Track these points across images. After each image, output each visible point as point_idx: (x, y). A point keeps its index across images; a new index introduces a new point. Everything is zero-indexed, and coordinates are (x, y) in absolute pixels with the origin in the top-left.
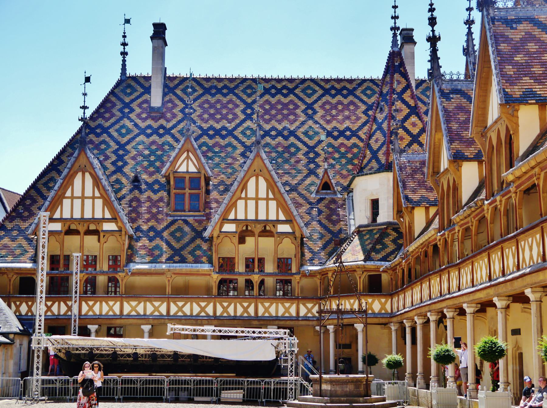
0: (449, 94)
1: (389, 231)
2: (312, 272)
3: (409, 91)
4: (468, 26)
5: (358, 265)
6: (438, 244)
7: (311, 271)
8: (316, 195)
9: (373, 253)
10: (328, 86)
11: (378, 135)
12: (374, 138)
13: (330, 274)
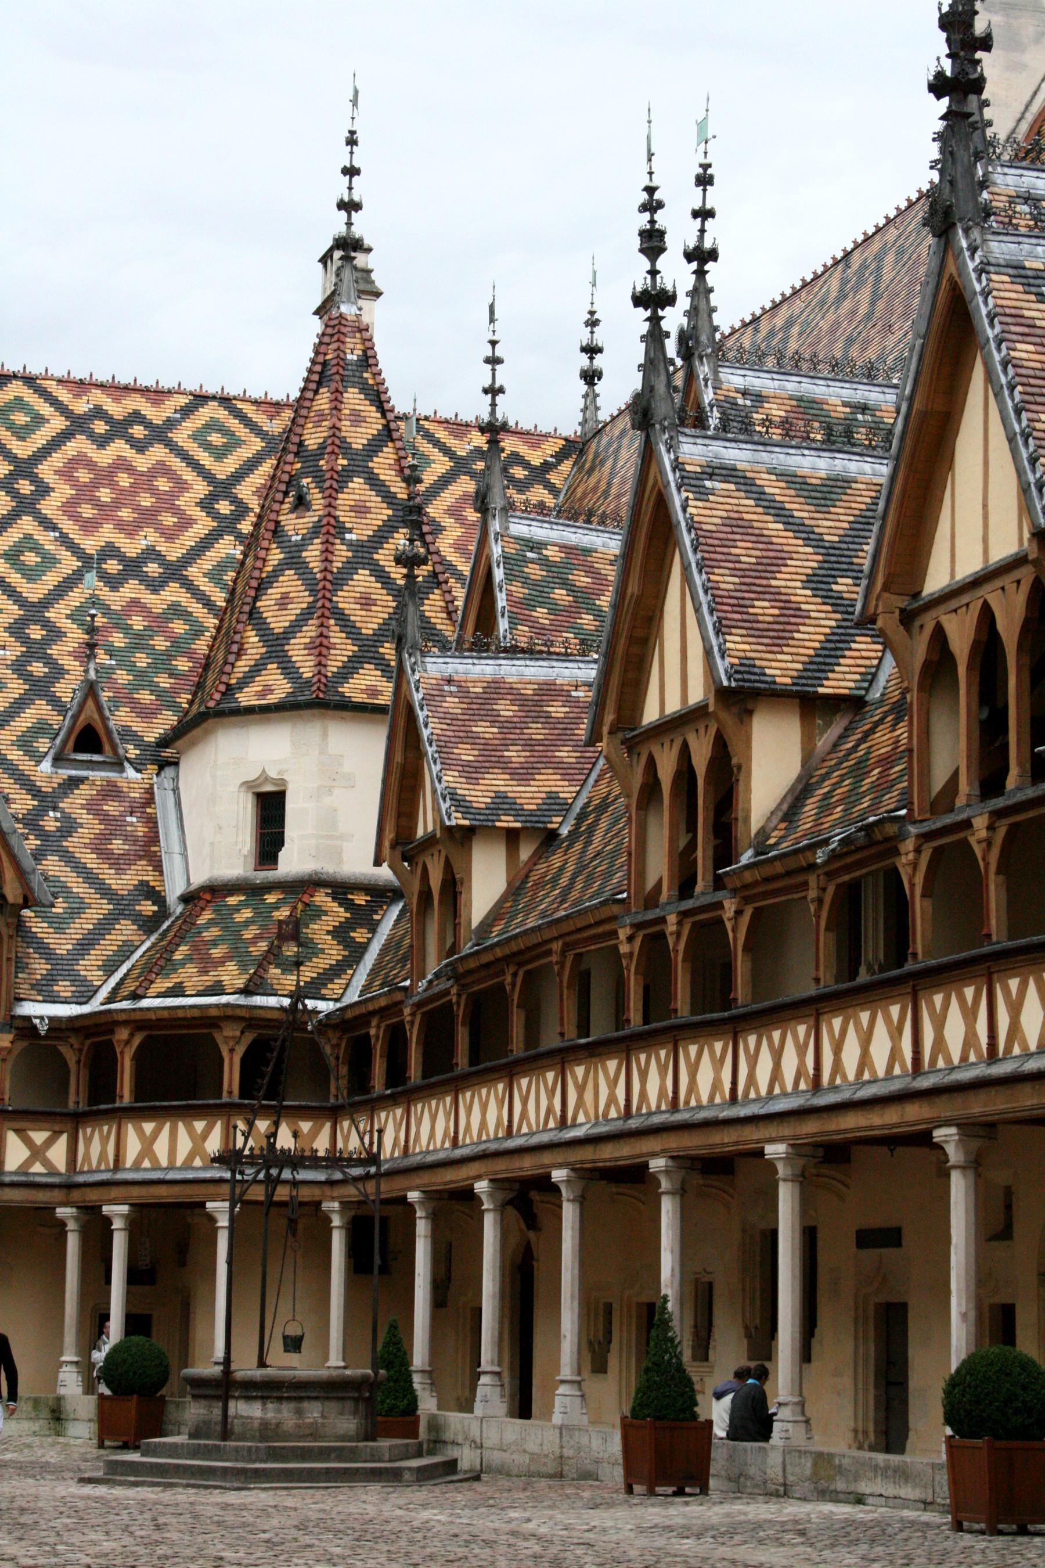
0: (700, 476)
1: (321, 898)
2: (56, 1025)
3: (389, 450)
4: (694, 265)
5: (227, 1005)
6: (624, 949)
7: (51, 1019)
8: (53, 766)
9: (274, 971)
10: (81, 407)
11: (289, 583)
12: (274, 593)
13: (123, 1034)
